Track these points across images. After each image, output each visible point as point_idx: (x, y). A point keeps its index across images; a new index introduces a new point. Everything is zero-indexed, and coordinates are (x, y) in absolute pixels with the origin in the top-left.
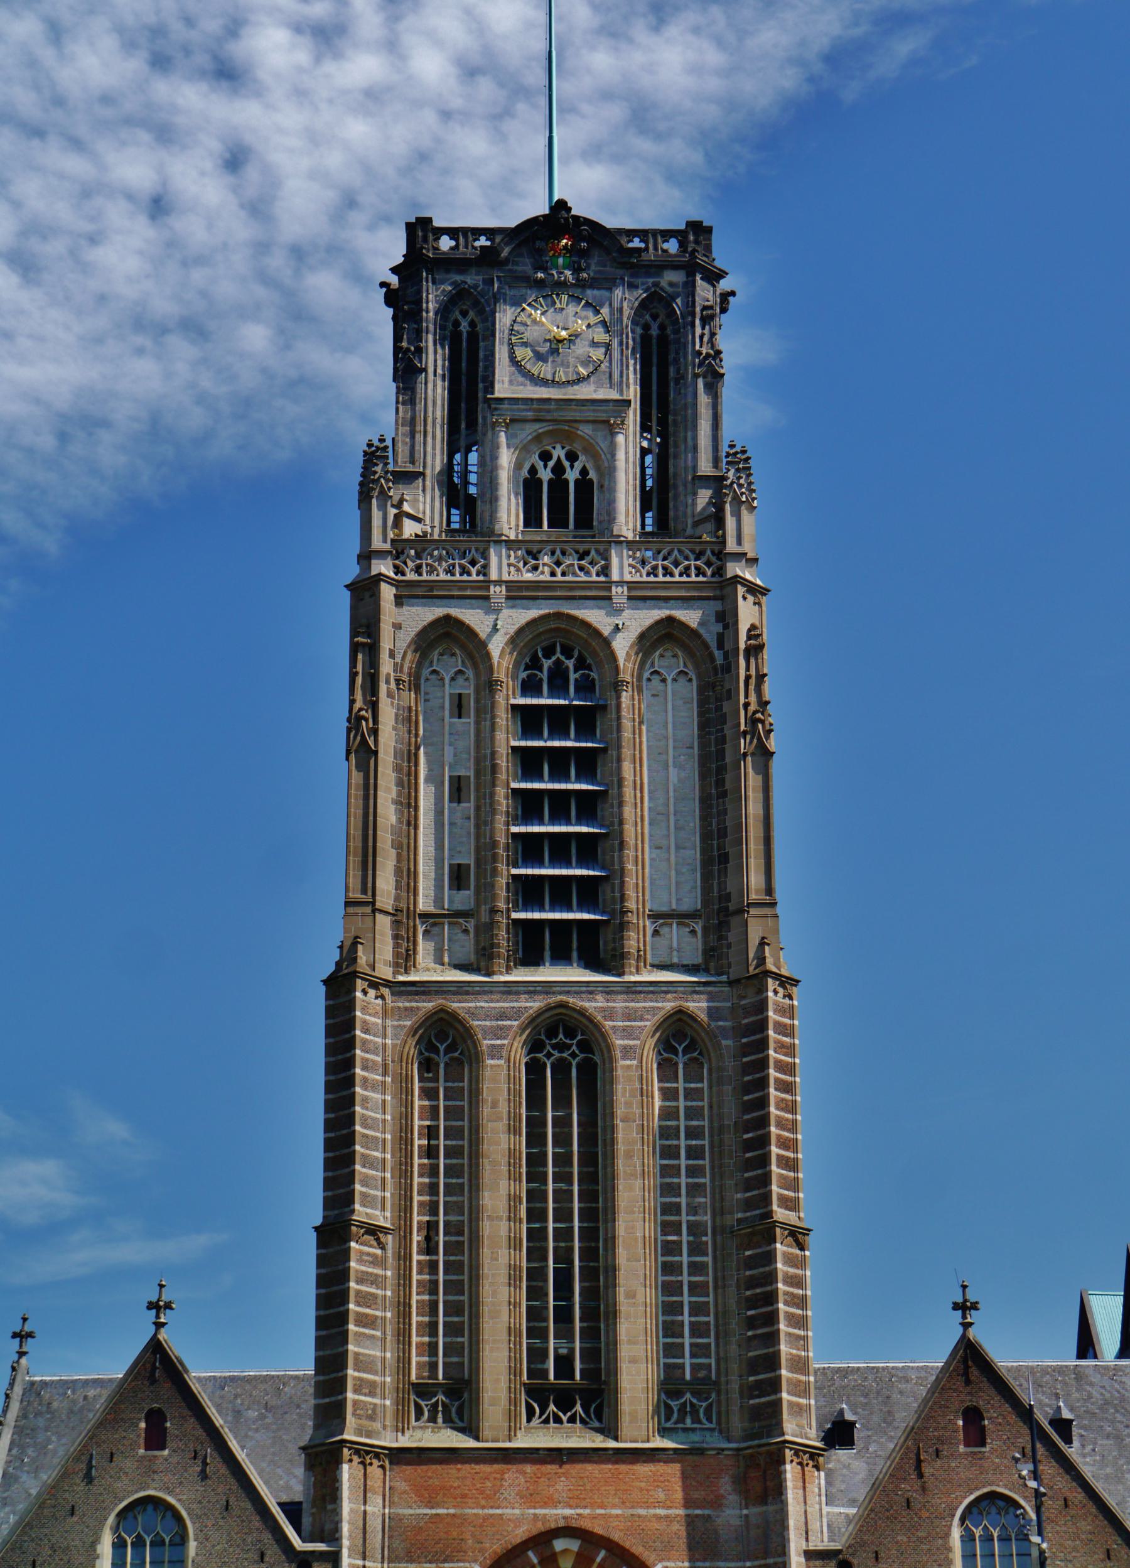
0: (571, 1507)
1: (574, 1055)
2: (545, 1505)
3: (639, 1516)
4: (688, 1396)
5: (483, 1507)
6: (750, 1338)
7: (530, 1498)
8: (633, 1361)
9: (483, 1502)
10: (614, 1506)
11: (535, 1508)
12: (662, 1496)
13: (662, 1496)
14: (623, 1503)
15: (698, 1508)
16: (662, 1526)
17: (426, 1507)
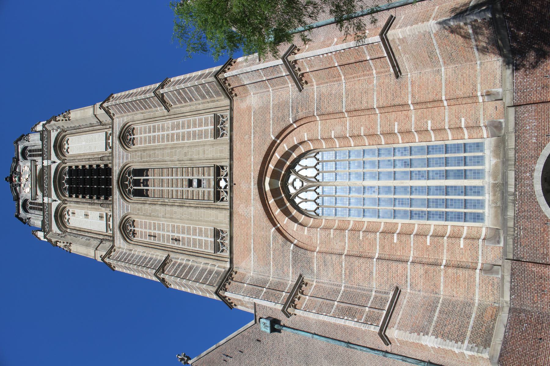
0: (251, 182)
1: (131, 178)
2: (250, 195)
3: (254, 147)
4: (219, 126)
5: (251, 225)
6: (195, 99)
7: (247, 202)
8: (204, 152)
9: (249, 225)
10: (250, 160)
11: (251, 200)
12: (247, 136)
13: (247, 136)
14: (249, 155)
15: (251, 118)
16: (257, 135)
17: (250, 253)
